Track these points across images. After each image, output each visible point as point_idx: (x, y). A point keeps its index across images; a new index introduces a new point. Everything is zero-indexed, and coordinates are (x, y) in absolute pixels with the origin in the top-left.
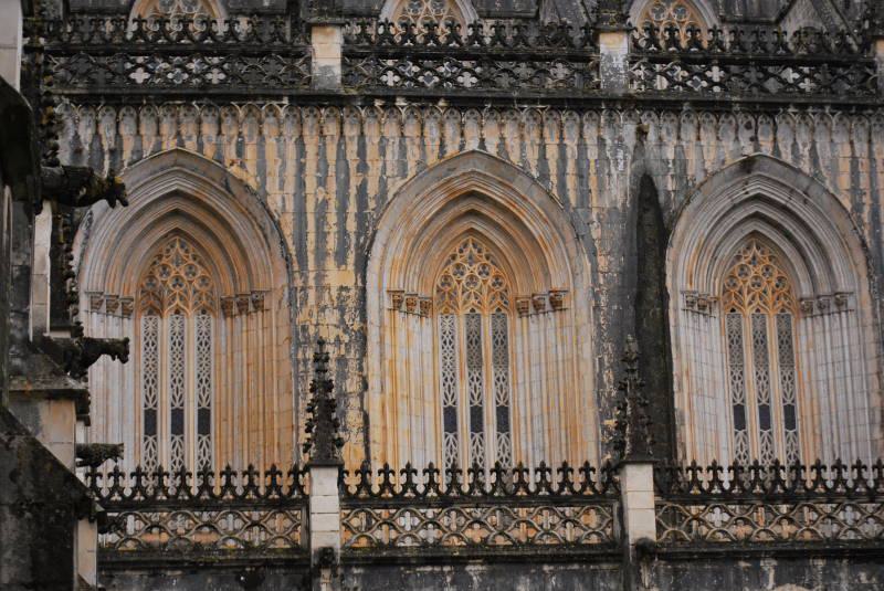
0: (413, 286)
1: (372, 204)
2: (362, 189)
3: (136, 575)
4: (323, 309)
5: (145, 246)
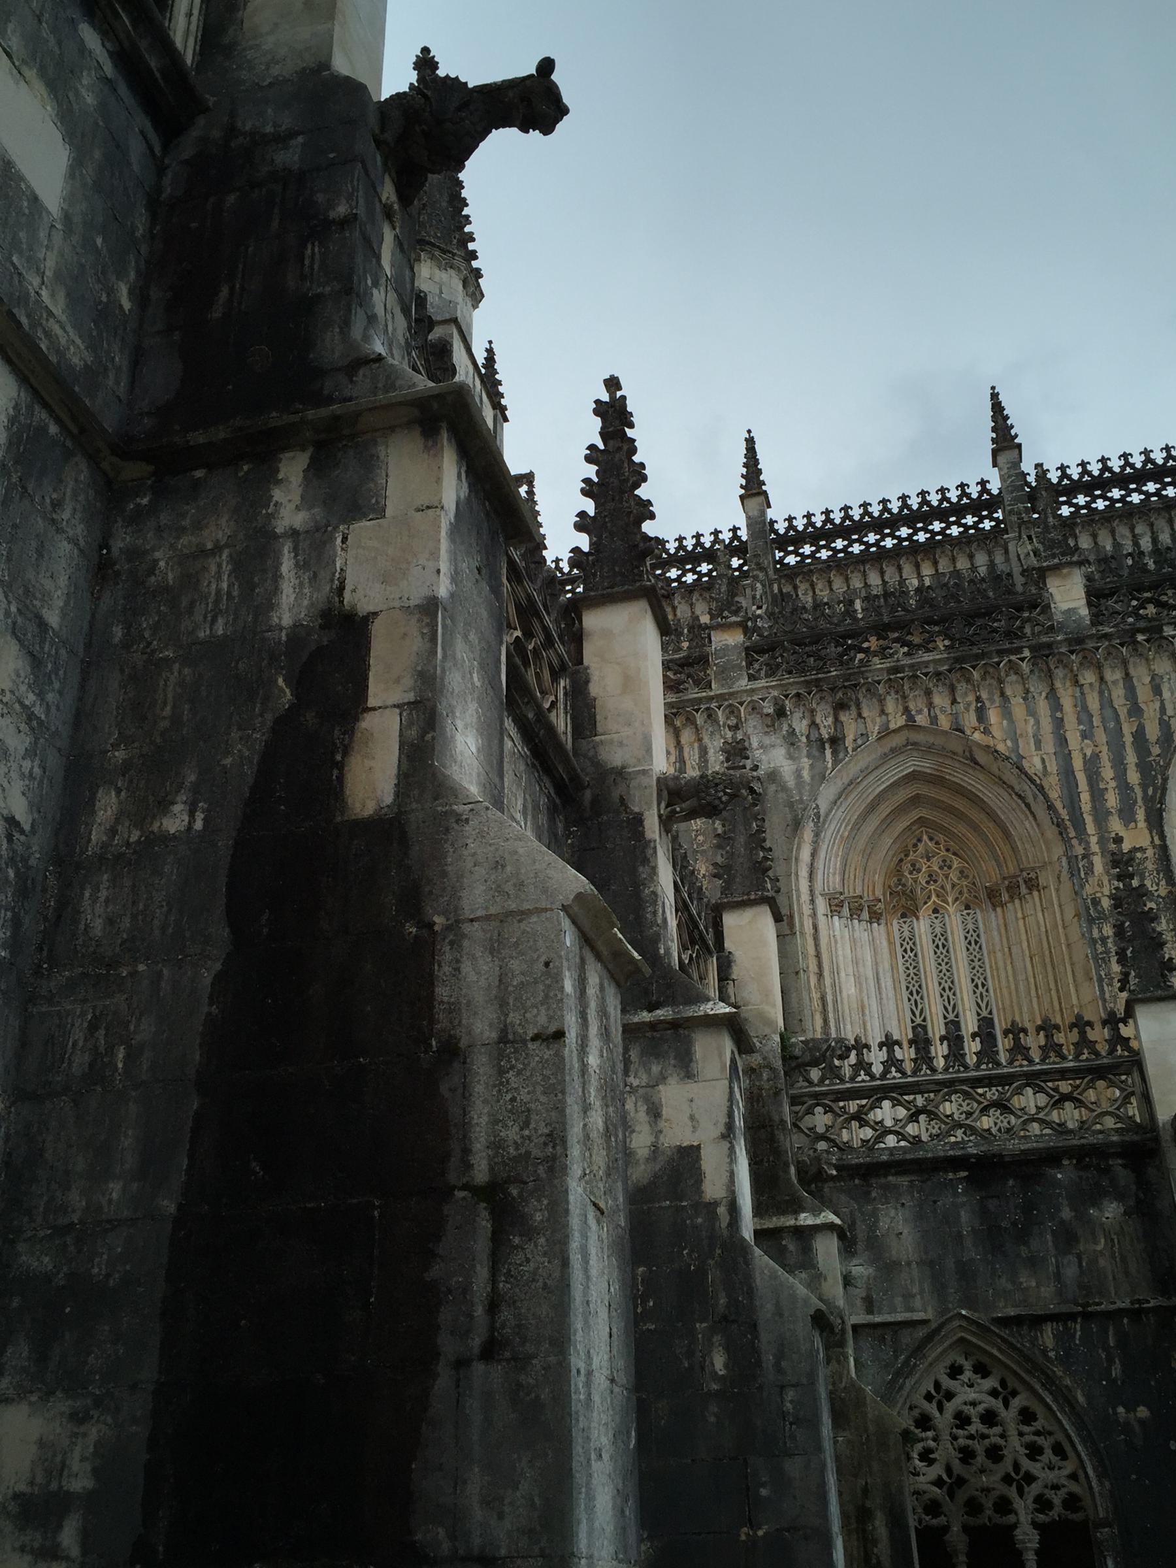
1: (1156, 750)
2: (1139, 736)
3: (904, 1181)
5: (887, 841)
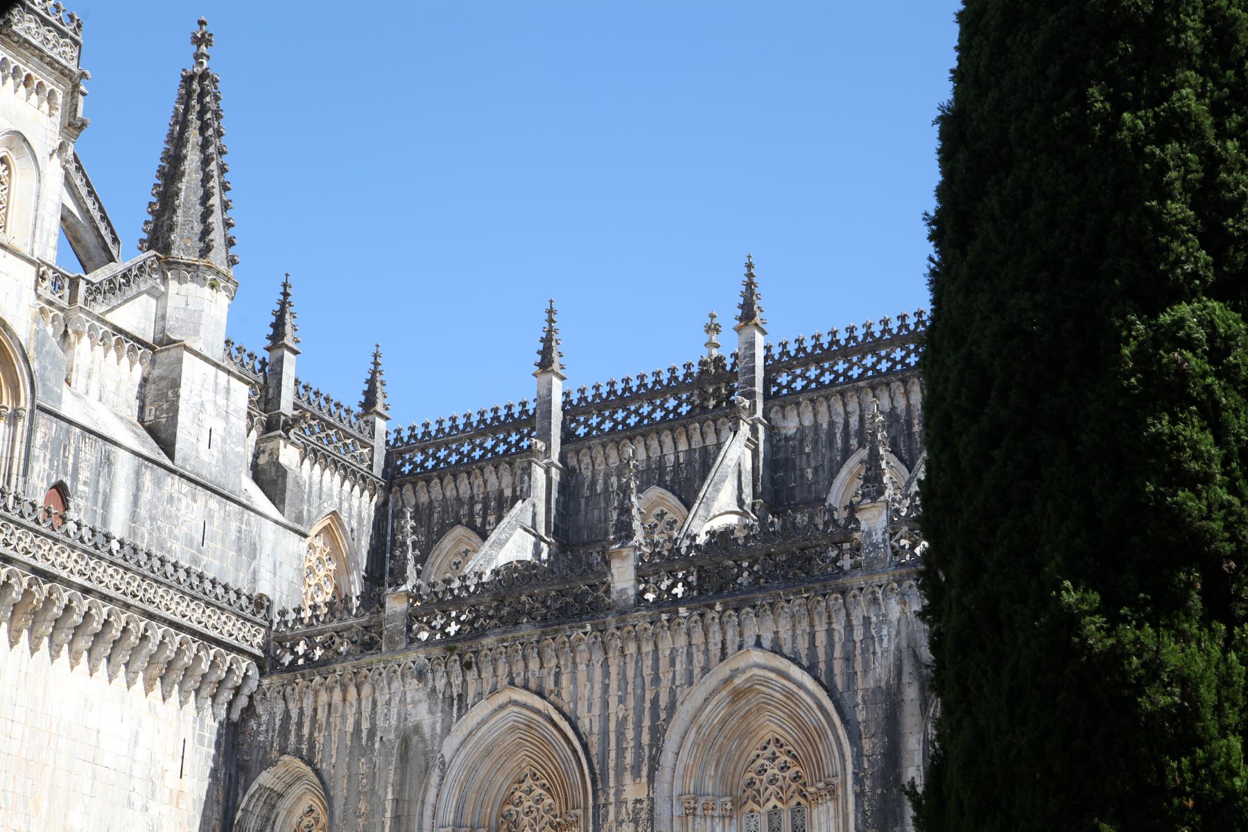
1: (663, 716)
2: (655, 702)
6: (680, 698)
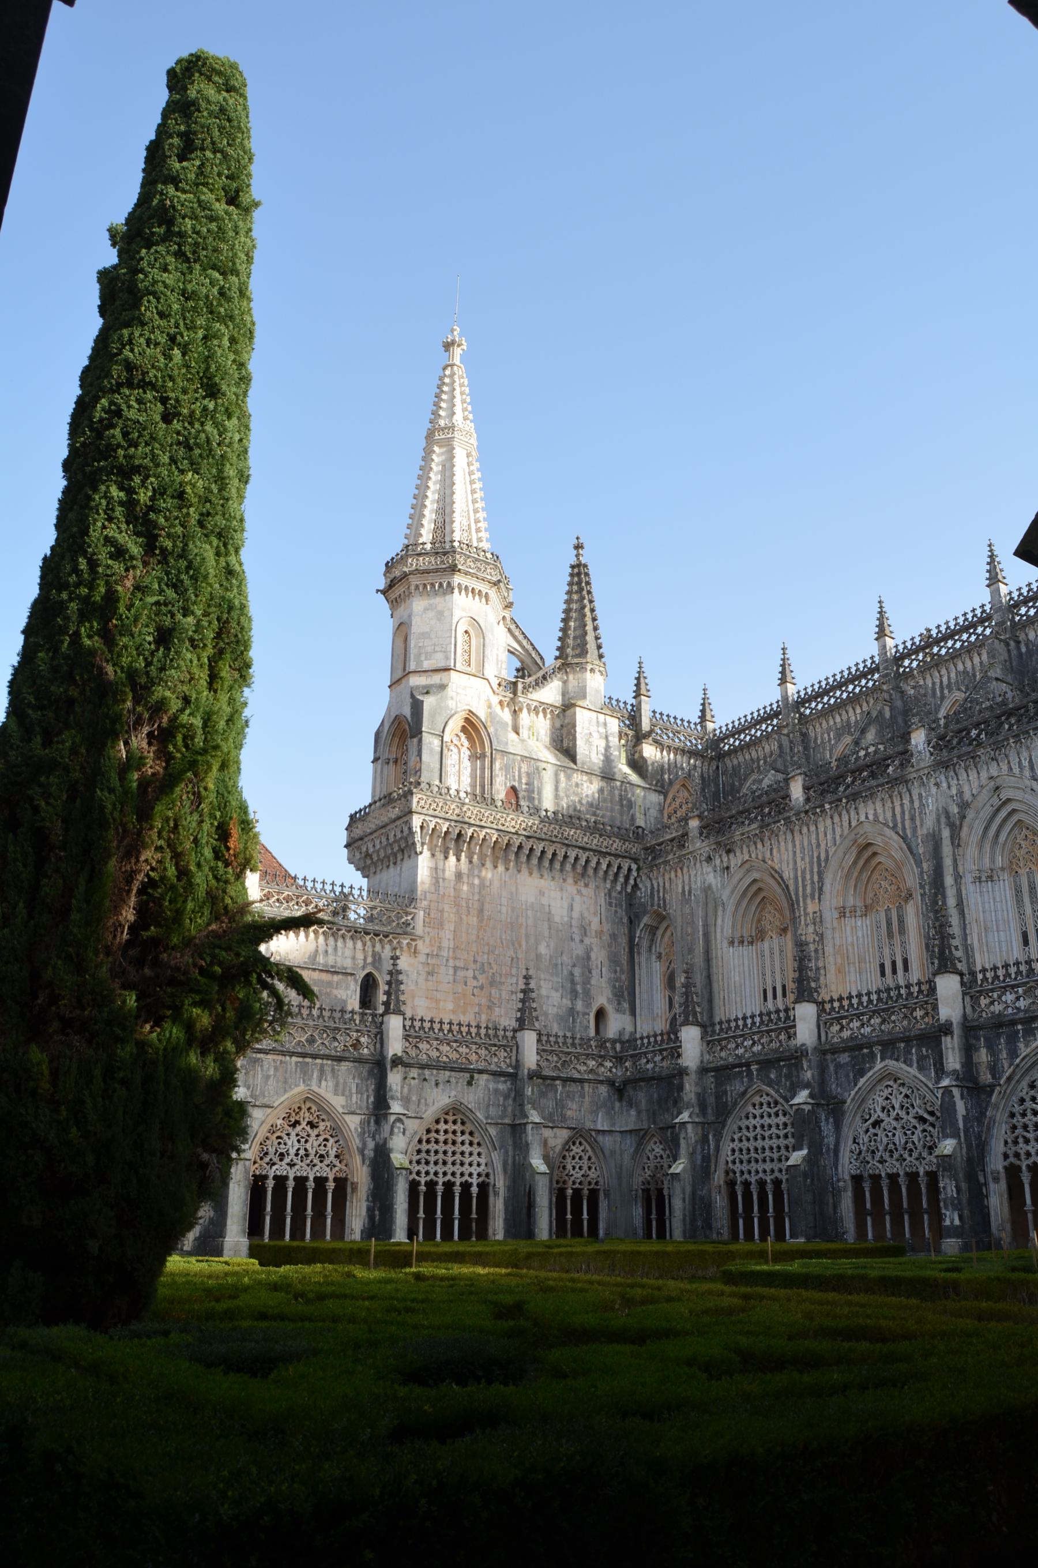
0: (851, 902)
1: (823, 864)
2: (819, 857)
4: (807, 925)
6: (831, 854)
